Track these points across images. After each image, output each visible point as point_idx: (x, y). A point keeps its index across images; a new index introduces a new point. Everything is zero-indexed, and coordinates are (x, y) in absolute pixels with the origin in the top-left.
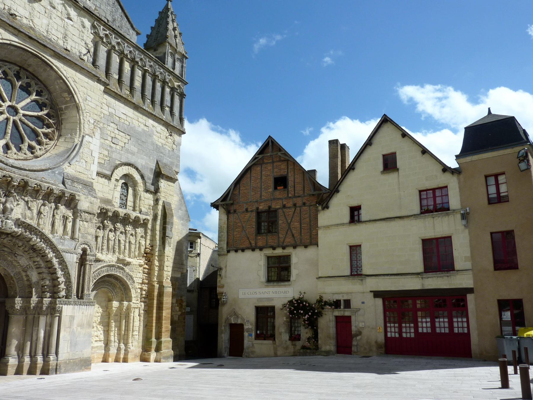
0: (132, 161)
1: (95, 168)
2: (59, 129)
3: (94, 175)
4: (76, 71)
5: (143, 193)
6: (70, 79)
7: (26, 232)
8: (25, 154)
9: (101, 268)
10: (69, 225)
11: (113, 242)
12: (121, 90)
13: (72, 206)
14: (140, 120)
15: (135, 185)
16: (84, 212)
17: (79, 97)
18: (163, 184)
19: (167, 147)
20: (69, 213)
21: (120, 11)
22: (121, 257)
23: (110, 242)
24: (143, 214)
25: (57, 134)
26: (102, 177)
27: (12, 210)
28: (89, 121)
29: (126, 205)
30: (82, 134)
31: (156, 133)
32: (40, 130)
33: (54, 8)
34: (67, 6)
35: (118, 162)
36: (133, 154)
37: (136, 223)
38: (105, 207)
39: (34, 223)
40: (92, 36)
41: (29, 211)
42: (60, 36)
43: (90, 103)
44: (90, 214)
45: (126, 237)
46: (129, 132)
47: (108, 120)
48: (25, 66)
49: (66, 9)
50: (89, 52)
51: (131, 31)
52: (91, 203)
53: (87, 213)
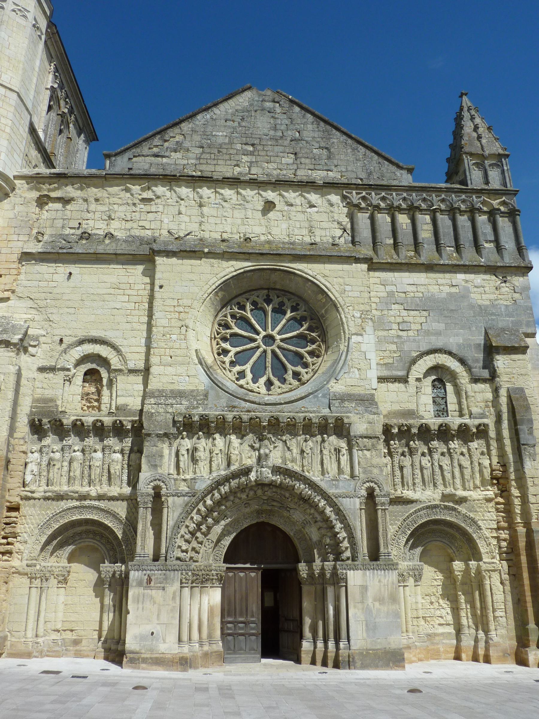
0: (439, 343)
1: (373, 374)
2: (324, 341)
3: (374, 383)
4: (324, 263)
5: (469, 386)
6: (318, 277)
7: (285, 480)
8: (290, 384)
9: (416, 512)
10: (344, 459)
12: (398, 255)
13: (345, 433)
14: (440, 281)
15: (453, 377)
16: (361, 437)
17: (334, 294)
18: (501, 362)
19: (501, 302)
20: (343, 444)
21: (376, 157)
23: (425, 471)
24: (476, 418)
25: (323, 347)
26: (392, 382)
27: (267, 455)
28: (353, 316)
29: (447, 411)
30: (347, 336)
31: (475, 289)
32: (302, 351)
33: (292, 205)
34: (305, 194)
35: (415, 354)
36: (438, 333)
37: (464, 434)
38: (405, 422)
40: (346, 210)
41: (289, 452)
42: (305, 232)
43: (350, 294)
44: (371, 438)
46: (427, 305)
47: (387, 304)
48: (272, 286)
49: (305, 198)
50: (345, 231)
51: (399, 173)
52: (370, 423)
53: (365, 437)
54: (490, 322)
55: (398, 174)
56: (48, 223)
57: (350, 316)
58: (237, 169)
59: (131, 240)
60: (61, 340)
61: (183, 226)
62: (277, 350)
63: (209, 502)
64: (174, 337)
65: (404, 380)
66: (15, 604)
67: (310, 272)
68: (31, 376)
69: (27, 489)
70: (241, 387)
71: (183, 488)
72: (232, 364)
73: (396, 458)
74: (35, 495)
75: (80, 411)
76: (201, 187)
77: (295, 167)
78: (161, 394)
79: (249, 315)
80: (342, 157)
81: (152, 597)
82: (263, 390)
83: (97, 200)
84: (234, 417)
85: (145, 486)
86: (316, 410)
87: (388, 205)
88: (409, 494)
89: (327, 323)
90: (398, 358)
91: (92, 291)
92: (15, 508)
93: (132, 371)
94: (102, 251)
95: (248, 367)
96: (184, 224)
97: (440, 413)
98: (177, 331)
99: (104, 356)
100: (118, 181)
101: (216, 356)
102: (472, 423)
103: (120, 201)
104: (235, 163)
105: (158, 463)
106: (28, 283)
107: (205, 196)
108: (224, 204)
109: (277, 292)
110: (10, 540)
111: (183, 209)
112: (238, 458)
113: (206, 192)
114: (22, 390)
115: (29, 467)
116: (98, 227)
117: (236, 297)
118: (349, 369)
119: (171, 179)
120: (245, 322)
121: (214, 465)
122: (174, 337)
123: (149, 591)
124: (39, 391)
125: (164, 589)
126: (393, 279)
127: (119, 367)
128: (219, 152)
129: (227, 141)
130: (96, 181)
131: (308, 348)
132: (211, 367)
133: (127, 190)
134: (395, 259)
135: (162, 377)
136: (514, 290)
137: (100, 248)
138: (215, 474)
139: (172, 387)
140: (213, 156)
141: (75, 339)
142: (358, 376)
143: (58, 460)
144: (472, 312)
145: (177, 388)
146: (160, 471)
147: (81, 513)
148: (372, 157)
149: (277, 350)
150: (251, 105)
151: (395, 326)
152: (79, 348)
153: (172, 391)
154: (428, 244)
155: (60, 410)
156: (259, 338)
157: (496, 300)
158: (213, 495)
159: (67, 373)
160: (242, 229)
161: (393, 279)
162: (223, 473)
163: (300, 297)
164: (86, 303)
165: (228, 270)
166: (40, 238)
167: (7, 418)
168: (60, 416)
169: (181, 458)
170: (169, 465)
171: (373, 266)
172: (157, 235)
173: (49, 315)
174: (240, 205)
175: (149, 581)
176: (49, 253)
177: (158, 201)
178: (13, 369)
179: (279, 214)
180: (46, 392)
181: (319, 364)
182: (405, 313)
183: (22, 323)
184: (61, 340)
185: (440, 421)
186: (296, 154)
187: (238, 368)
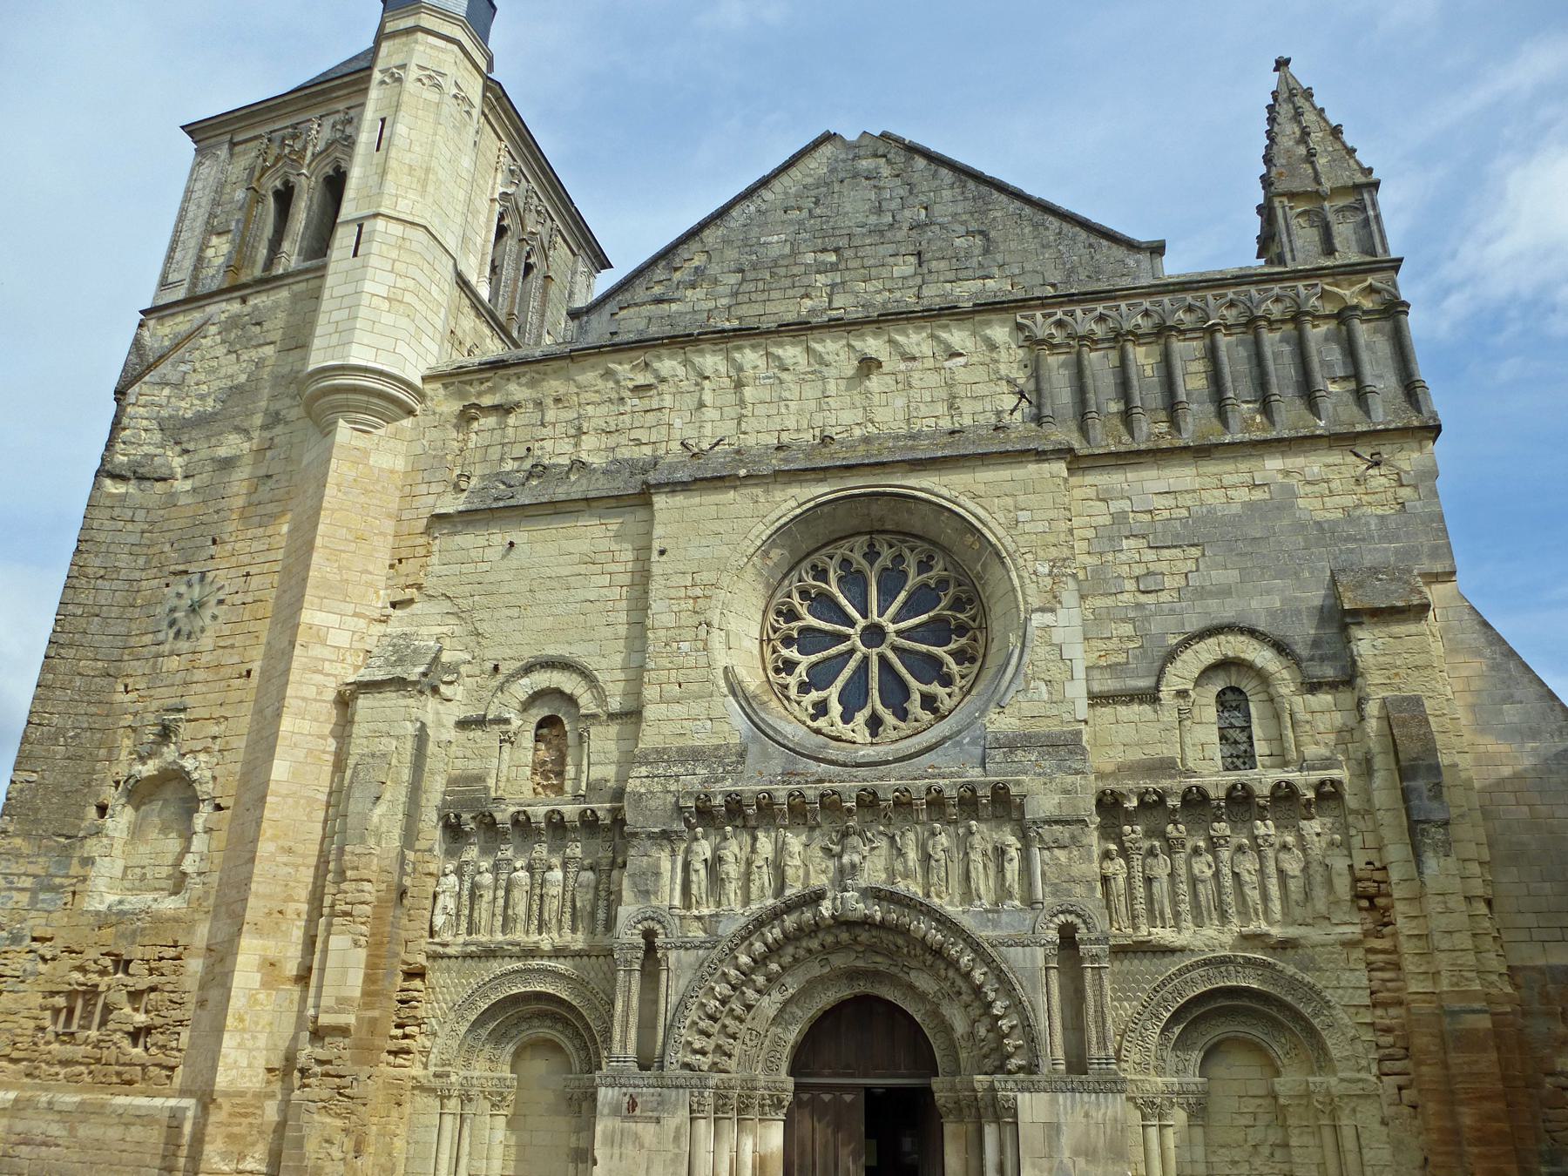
0: (1226, 611)
1: (1077, 691)
3: (1082, 710)
6: (962, 499)
10: (1012, 869)
11: (1211, 885)
18: (1367, 643)
21: (1083, 235)
22: (1259, 925)
23: (1200, 887)
24: (1314, 769)
26: (1126, 703)
28: (1035, 573)
31: (1308, 489)
33: (914, 359)
35: (1173, 641)
36: (1225, 592)
38: (1151, 785)
39: (915, 889)
42: (941, 409)
43: (1028, 527)
44: (1067, 823)
45: (1262, 858)
46: (1197, 534)
47: (1111, 539)
48: (877, 526)
50: (1023, 396)
52: (1066, 792)
53: (1057, 822)
54: (1344, 557)
55: (1132, 263)
56: (478, 456)
57: (1027, 575)
58: (808, 303)
59: (616, 467)
60: (496, 668)
61: (708, 430)
62: (891, 655)
63: (744, 959)
65: (1150, 697)
66: (417, 1143)
68: (445, 736)
70: (818, 732)
71: (696, 933)
72: (804, 688)
73: (1137, 863)
74: (450, 951)
75: (529, 794)
76: (739, 348)
77: (919, 280)
78: (660, 755)
80: (1013, 245)
81: (637, 1137)
82: (863, 735)
83: (557, 400)
84: (791, 795)
85: (628, 933)
86: (955, 771)
87: (1112, 330)
88: (1164, 935)
89: (989, 590)
90: (1137, 652)
91: (549, 572)
92: (420, 974)
94: (563, 497)
95: (833, 693)
96: (709, 426)
97: (1238, 762)
98: (690, 634)
99: (568, 691)
100: (593, 360)
101: (771, 674)
103: (596, 398)
104: (803, 291)
106: (444, 570)
107: (747, 366)
108: (784, 376)
109: (888, 537)
110: (408, 1030)
111: (708, 397)
112: (801, 872)
113: (750, 357)
114: (429, 764)
115: (441, 897)
116: (557, 451)
117: (808, 555)
118: (1028, 683)
119: (682, 341)
120: (824, 604)
121: (754, 889)
122: (685, 646)
123: (633, 1125)
124: (459, 763)
125: (658, 1121)
126: (1125, 486)
127: (593, 709)
129: (787, 250)
130: (555, 364)
131: (952, 646)
132: (755, 697)
133: (608, 374)
134: (1127, 444)
135: (664, 723)
136: (1400, 479)
137: (559, 490)
138: (754, 906)
140: (760, 284)
141: (519, 664)
142: (1045, 697)
143: (488, 887)
144: (1300, 539)
145: (690, 743)
147: (526, 982)
148: (1075, 235)
149: (891, 655)
150: (832, 171)
151: (1130, 585)
153: (680, 750)
154: (1201, 403)
155: (493, 795)
156: (854, 633)
157: (1357, 507)
158: (751, 944)
159: (504, 727)
160: (818, 420)
161: (1125, 486)
162: (770, 902)
163: (933, 543)
164: (537, 595)
165: (785, 507)
166: (463, 485)
167: (400, 816)
169: (694, 877)
170: (672, 890)
171: (1077, 462)
172: (661, 452)
173: (477, 625)
174: (812, 373)
175: (633, 1105)
176: (476, 511)
177: (663, 387)
178: (411, 728)
179: (889, 380)
180: (471, 764)
181: (973, 676)
182: (1150, 555)
184: (496, 668)
185: (1232, 777)
187: (815, 695)
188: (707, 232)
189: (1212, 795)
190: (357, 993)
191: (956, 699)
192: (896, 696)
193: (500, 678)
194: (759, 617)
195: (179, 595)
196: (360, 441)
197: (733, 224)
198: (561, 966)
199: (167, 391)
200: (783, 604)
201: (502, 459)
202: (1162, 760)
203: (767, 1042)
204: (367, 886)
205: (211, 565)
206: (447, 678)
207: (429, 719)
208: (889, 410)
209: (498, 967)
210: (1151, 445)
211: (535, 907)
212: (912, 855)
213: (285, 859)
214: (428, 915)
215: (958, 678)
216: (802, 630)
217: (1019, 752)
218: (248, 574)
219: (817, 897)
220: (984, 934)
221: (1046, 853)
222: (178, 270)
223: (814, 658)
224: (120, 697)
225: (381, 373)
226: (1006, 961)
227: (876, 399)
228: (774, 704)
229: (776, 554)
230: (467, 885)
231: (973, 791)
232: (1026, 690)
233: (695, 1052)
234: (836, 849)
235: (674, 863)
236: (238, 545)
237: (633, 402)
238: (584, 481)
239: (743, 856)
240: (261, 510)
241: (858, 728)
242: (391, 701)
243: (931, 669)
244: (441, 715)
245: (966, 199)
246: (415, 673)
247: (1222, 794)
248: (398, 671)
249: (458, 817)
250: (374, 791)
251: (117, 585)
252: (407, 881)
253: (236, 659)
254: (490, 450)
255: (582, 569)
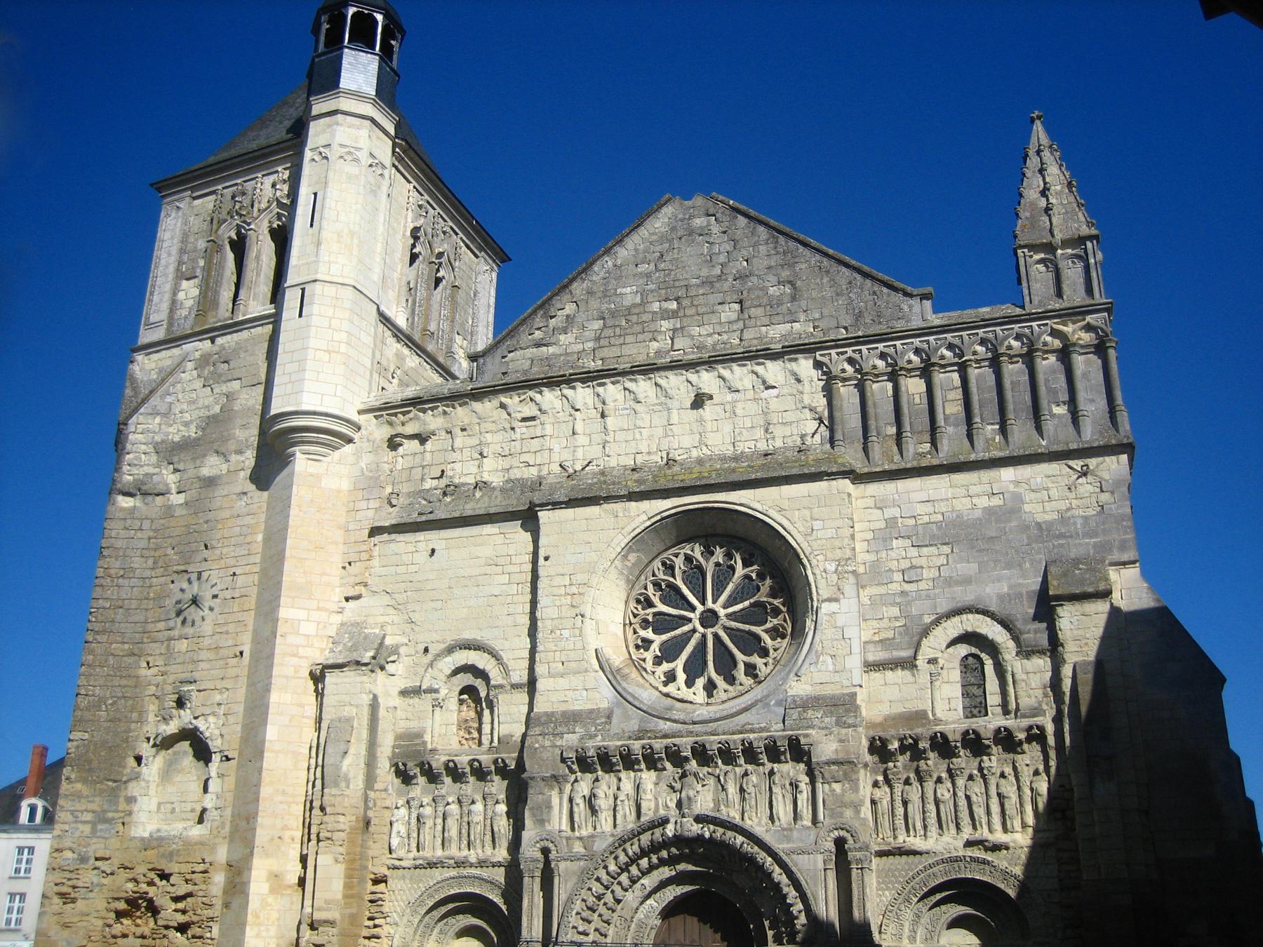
0: (968, 596)
1: (854, 663)
3: (857, 675)
10: (803, 798)
17: (796, 536)
19: (1075, 512)
23: (942, 806)
28: (825, 571)
31: (1033, 495)
32: (757, 630)
35: (928, 619)
36: (967, 581)
39: (734, 815)
42: (759, 433)
43: (820, 534)
46: (952, 533)
47: (884, 540)
54: (1056, 551)
55: (906, 308)
57: (820, 573)
58: (655, 345)
59: (513, 486)
60: (426, 650)
64: (566, 633)
65: (909, 664)
67: (759, 507)
68: (391, 704)
69: (394, 856)
70: (667, 695)
71: (578, 848)
72: (658, 661)
73: (898, 788)
76: (603, 384)
77: (741, 324)
79: (679, 582)
80: (814, 294)
86: (767, 724)
88: (916, 842)
93: (515, 686)
95: (679, 664)
96: (580, 450)
97: (975, 711)
98: (569, 623)
99: (481, 667)
101: (632, 650)
102: (1017, 725)
104: (650, 335)
105: (545, 817)
106: (383, 571)
108: (638, 407)
110: (377, 922)
113: (612, 391)
115: (395, 825)
116: (464, 472)
118: (818, 658)
120: (672, 595)
122: (566, 633)
126: (896, 496)
128: (628, 321)
129: (638, 300)
131: (768, 625)
132: (619, 670)
134: (898, 463)
137: (468, 506)
139: (563, 707)
140: (618, 330)
141: (443, 646)
142: (831, 668)
143: (429, 817)
145: (572, 708)
146: (548, 827)
150: (673, 229)
151: (898, 577)
152: (448, 659)
153: (564, 713)
154: (956, 426)
155: (429, 747)
156: (695, 616)
157: (1068, 510)
161: (896, 496)
162: (631, 826)
164: (455, 591)
168: (428, 757)
169: (576, 809)
170: (560, 819)
171: (857, 477)
172: (545, 472)
173: (411, 615)
174: (660, 404)
177: (543, 418)
178: (366, 699)
179: (719, 409)
182: (913, 552)
183: (377, 631)
184: (426, 650)
186: (741, 302)
187: (666, 666)
188: (575, 285)
189: (951, 738)
190: (339, 896)
191: (770, 667)
192: (726, 666)
193: (430, 656)
194: (622, 606)
195: (182, 590)
196: (313, 468)
197: (594, 278)
198: (484, 873)
199: (158, 420)
200: (641, 594)
201: (423, 479)
202: (917, 712)
203: (633, 925)
204: (341, 818)
205: (204, 566)
206: (392, 659)
207: (379, 691)
208: (719, 435)
209: (438, 874)
210: (915, 464)
211: (464, 831)
212: (732, 789)
213: (280, 798)
214: (387, 838)
215: (771, 651)
216: (655, 614)
217: (810, 712)
218: (234, 574)
219: (665, 821)
220: (779, 847)
221: (826, 786)
222: (158, 311)
223: (664, 637)
224: (144, 672)
225: (327, 415)
226: (796, 865)
227: (709, 426)
228: (634, 674)
229: (632, 557)
230: (414, 816)
231: (775, 742)
232: (816, 663)
233: (580, 933)
234: (678, 786)
235: (561, 799)
236: (225, 551)
237: (522, 429)
238: (486, 499)
239: (611, 793)
240: (240, 521)
241: (698, 693)
242: (348, 676)
243: (752, 644)
244: (387, 686)
245: (778, 253)
246: (367, 656)
247: (958, 737)
248: (355, 656)
249: (405, 765)
250: (342, 747)
251: (134, 582)
252: (370, 814)
253: (230, 643)
254: (414, 471)
255: (488, 570)
